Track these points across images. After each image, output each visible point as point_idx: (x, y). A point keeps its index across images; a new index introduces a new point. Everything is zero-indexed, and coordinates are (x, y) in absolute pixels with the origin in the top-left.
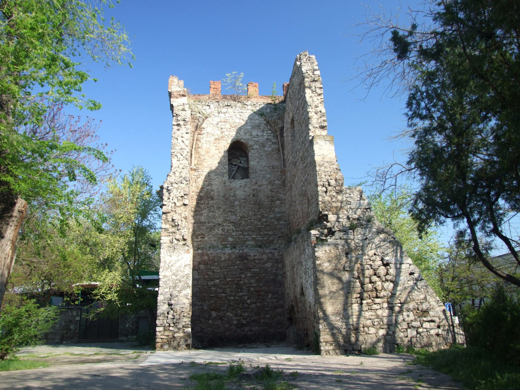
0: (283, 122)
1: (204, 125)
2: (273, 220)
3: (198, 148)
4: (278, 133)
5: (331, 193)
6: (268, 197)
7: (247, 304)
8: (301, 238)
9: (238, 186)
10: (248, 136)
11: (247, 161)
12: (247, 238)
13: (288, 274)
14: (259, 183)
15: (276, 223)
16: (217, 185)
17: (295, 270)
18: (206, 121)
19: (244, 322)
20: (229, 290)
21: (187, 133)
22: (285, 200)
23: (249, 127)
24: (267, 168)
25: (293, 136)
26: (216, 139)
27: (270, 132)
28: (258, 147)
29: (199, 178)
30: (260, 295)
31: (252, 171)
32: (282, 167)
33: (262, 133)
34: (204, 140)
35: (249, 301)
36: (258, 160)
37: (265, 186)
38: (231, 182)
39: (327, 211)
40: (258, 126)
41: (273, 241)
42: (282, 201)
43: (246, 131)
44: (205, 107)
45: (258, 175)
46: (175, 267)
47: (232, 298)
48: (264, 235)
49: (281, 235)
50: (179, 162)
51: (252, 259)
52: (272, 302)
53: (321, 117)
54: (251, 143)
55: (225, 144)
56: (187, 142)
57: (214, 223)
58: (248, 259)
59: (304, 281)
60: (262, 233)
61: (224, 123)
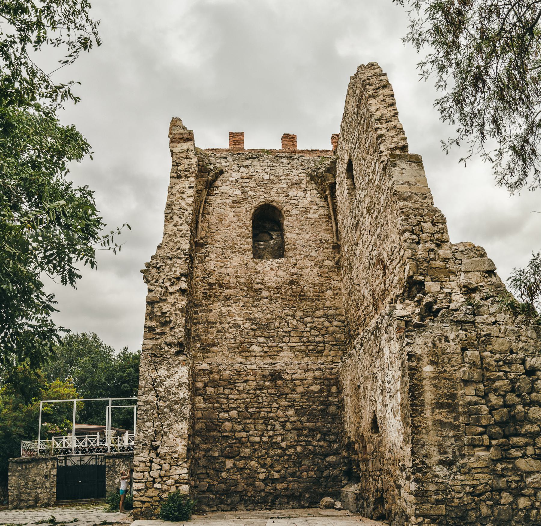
0: (334, 176)
1: (218, 183)
2: (322, 320)
3: (208, 213)
4: (327, 192)
5: (427, 245)
6: (314, 285)
7: (281, 448)
8: (372, 333)
9: (268, 269)
10: (282, 198)
12: (281, 347)
14: (301, 264)
15: (327, 324)
16: (234, 267)
17: (361, 390)
18: (220, 178)
19: (276, 475)
20: (252, 426)
21: (190, 187)
22: (340, 289)
23: (285, 186)
24: (311, 243)
25: (353, 187)
26: (234, 202)
27: (316, 192)
28: (298, 212)
31: (289, 247)
33: (303, 194)
34: (217, 202)
35: (283, 444)
36: (297, 231)
38: (256, 263)
39: (421, 274)
40: (296, 184)
41: (322, 351)
42: (336, 292)
43: (280, 191)
44: (219, 160)
45: (298, 252)
46: (163, 387)
47: (257, 439)
48: (309, 342)
50: (176, 229)
54: (287, 207)
56: (190, 200)
57: (229, 323)
58: (281, 379)
59: (379, 407)
60: (305, 340)
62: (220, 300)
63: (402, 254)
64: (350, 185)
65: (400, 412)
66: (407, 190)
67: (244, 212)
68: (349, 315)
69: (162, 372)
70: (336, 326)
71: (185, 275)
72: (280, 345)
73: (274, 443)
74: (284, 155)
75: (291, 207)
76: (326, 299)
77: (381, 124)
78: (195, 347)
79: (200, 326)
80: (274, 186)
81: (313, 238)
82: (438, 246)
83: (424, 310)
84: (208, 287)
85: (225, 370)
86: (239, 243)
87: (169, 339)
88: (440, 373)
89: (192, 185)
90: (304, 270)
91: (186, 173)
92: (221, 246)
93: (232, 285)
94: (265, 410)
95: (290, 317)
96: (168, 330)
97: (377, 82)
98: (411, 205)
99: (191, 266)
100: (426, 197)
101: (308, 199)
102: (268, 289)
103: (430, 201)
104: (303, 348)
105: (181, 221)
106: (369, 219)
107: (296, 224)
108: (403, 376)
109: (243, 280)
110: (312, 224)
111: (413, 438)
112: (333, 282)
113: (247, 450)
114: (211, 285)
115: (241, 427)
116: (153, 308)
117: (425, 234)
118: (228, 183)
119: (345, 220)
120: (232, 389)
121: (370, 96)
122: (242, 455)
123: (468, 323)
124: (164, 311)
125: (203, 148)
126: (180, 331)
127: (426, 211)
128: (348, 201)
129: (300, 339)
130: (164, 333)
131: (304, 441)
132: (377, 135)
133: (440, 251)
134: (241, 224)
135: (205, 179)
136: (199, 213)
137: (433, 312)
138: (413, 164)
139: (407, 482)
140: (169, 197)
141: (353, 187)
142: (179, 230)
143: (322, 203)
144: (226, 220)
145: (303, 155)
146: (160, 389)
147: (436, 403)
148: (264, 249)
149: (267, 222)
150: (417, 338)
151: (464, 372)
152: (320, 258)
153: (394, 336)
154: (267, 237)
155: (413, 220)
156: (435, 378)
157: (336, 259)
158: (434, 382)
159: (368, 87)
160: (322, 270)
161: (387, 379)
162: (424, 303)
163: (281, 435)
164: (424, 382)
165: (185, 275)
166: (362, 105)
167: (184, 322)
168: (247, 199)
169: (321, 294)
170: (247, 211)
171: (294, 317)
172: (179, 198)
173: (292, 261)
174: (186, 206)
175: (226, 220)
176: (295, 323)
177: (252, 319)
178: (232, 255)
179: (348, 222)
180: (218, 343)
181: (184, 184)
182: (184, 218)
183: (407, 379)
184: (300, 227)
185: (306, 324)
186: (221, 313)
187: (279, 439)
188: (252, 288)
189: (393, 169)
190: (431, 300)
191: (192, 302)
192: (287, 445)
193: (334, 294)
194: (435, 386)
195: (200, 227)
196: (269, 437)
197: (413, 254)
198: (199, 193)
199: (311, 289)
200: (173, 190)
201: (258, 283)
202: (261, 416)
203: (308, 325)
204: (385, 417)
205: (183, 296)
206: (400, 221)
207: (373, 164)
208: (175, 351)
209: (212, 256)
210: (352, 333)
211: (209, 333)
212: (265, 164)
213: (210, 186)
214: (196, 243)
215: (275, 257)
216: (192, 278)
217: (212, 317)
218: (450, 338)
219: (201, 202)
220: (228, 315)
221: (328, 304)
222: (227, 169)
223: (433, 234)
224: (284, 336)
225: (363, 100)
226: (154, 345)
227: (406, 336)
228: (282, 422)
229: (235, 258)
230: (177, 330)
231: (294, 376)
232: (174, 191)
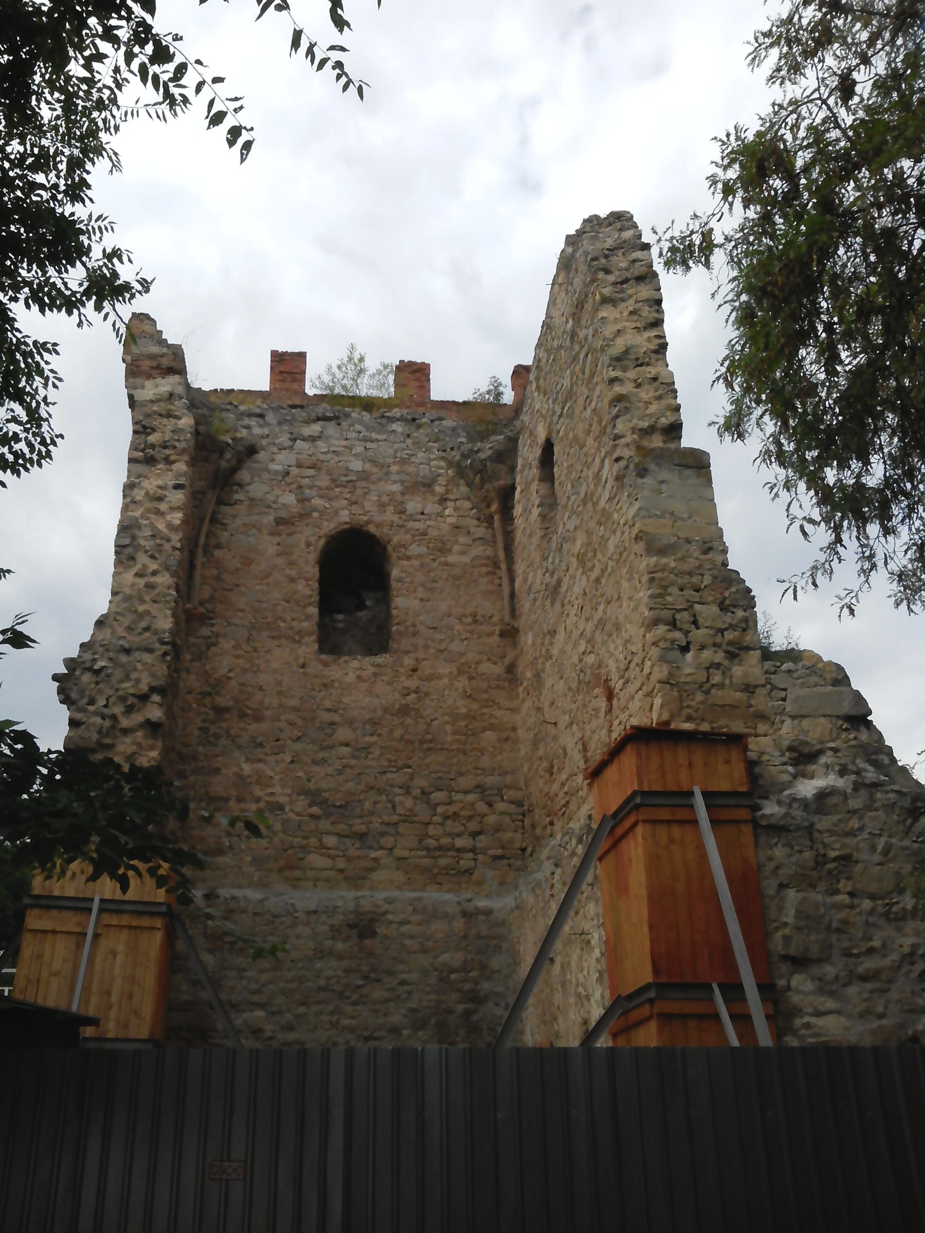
0: (512, 469)
2: (471, 797)
4: (494, 507)
9: (351, 678)
10: (390, 515)
14: (426, 668)
15: (481, 807)
22: (514, 729)
23: (396, 488)
25: (550, 504)
27: (467, 504)
28: (424, 550)
29: (215, 644)
31: (401, 628)
32: (507, 618)
33: (437, 508)
36: (421, 593)
37: (445, 681)
38: (326, 664)
40: (424, 485)
42: (505, 735)
43: (385, 498)
45: (421, 642)
48: (440, 848)
49: (499, 852)
55: (312, 539)
60: (431, 842)
62: (239, 748)
67: (303, 545)
70: (502, 813)
72: (373, 854)
75: (408, 537)
76: (482, 751)
80: (373, 487)
84: (212, 715)
86: (288, 617)
90: (434, 683)
95: (398, 791)
101: (449, 520)
102: (351, 723)
104: (426, 862)
106: (582, 583)
109: (294, 703)
110: (456, 578)
112: (499, 713)
114: (220, 711)
118: (266, 476)
121: (605, 300)
125: (206, 387)
129: (420, 841)
132: (610, 395)
134: (293, 573)
141: (550, 504)
143: (481, 532)
145: (443, 414)
149: (354, 571)
157: (508, 660)
159: (601, 275)
166: (585, 317)
168: (304, 516)
169: (471, 739)
170: (308, 544)
171: (407, 790)
173: (408, 661)
176: (409, 803)
179: (538, 579)
180: (230, 847)
188: (313, 719)
201: (329, 710)
203: (440, 809)
207: (598, 460)
209: (226, 645)
210: (538, 831)
214: (187, 612)
220: (258, 783)
221: (485, 761)
222: (264, 442)
224: (383, 834)
225: (588, 306)
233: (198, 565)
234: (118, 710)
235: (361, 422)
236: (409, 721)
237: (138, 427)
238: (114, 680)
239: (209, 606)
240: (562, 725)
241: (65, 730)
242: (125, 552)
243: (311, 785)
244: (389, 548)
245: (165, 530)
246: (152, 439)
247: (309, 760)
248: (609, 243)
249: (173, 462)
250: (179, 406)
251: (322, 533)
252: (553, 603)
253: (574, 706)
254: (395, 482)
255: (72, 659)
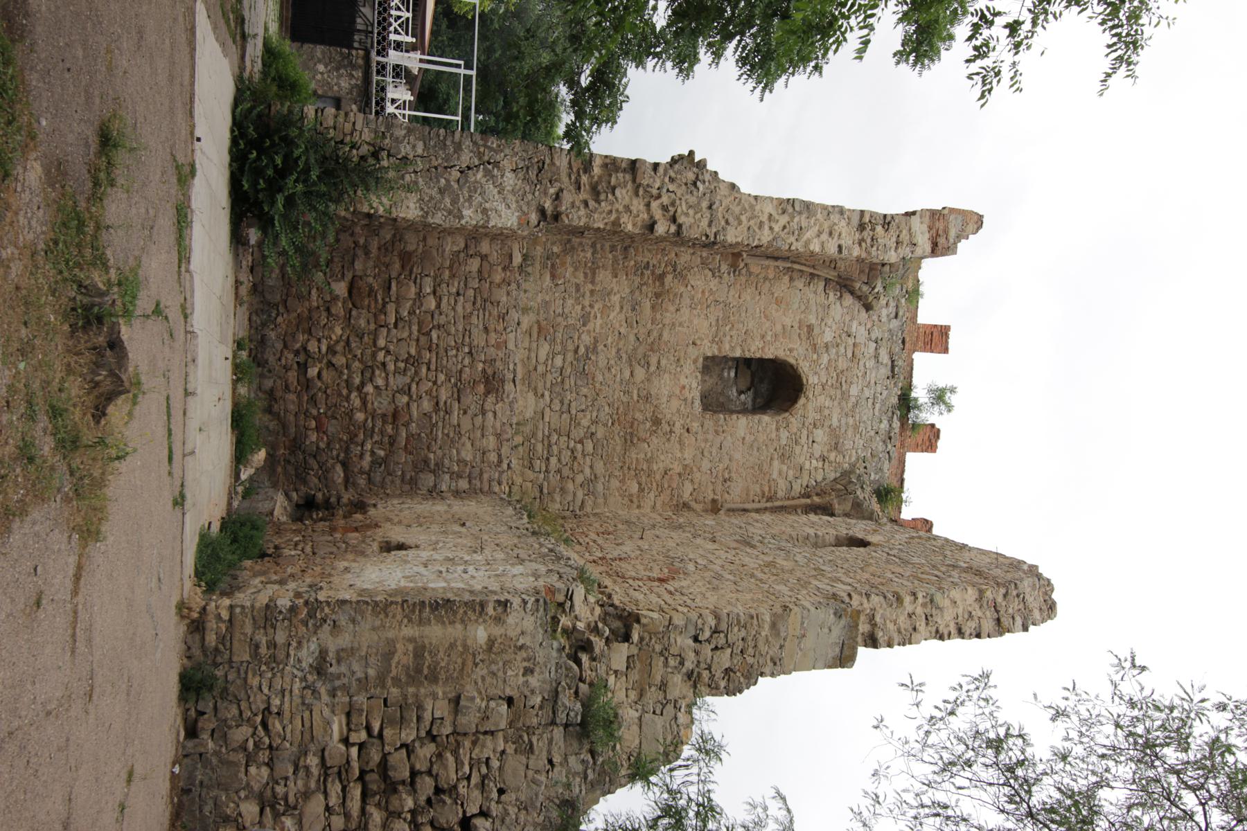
0: (847, 515)
1: (848, 300)
2: (587, 471)
3: (791, 279)
4: (817, 499)
5: (692, 655)
7: (363, 384)
8: (551, 550)
9: (683, 381)
10: (812, 416)
11: (744, 411)
12: (543, 395)
13: (440, 507)
14: (689, 440)
15: (580, 479)
16: (691, 322)
17: (457, 528)
19: (313, 372)
20: (405, 335)
21: (840, 247)
22: (639, 507)
23: (835, 423)
24: (727, 462)
26: (810, 328)
27: (819, 479)
28: (784, 442)
30: (384, 422)
32: (727, 506)
34: (811, 296)
35: (369, 388)
36: (749, 438)
37: (679, 455)
38: (695, 362)
39: (641, 639)
41: (531, 467)
42: (635, 500)
43: (826, 412)
44: (892, 304)
45: (710, 437)
47: (381, 342)
48: (550, 446)
49: (545, 491)
50: (765, 218)
51: (487, 407)
52: (361, 456)
53: (900, 632)
56: (815, 247)
57: (591, 306)
58: (487, 393)
59: (425, 555)
61: (850, 355)
63: (680, 608)
64: (824, 540)
65: (412, 585)
66: (791, 631)
67: (790, 346)
68: (592, 518)
69: (509, 179)
70: (575, 494)
71: (678, 233)
72: (547, 394)
73: (373, 373)
74: (894, 425)
76: (622, 481)
77: (924, 605)
78: (553, 244)
79: (589, 255)
80: (836, 403)
81: (734, 466)
82: (689, 675)
83: (580, 637)
84: (658, 272)
85: (508, 294)
86: (733, 333)
87: (567, 198)
88: (474, 655)
89: (845, 252)
91: (869, 241)
92: (731, 299)
93: (658, 316)
94: (434, 360)
95: (595, 414)
96: (584, 195)
97: (1010, 611)
98: (763, 634)
99: (694, 244)
100: (775, 664)
101: (807, 463)
103: (767, 670)
104: (540, 435)
105: (777, 228)
107: (762, 437)
108: (471, 592)
110: (760, 467)
111: (367, 603)
112: (652, 495)
113: (362, 323)
114: (661, 277)
115: (406, 314)
116: (625, 171)
117: (710, 654)
118: (848, 318)
119: (759, 526)
120: (474, 303)
122: (354, 313)
123: (554, 713)
124: (617, 192)
126: (579, 218)
127: (750, 660)
128: (794, 534)
130: (579, 188)
131: (374, 426)
133: (680, 677)
135: (856, 275)
136: (793, 262)
137: (576, 653)
138: (838, 650)
139: (292, 594)
140: (825, 207)
142: (761, 225)
143: (797, 488)
144: (777, 311)
145: (895, 462)
146: (480, 175)
147: (424, 647)
148: (721, 377)
150: (532, 619)
151: (473, 699)
152: (698, 475)
153: (541, 583)
154: (744, 384)
155: (736, 635)
156: (465, 646)
157: (693, 504)
158: (458, 643)
160: (676, 478)
161: (471, 569)
162: (592, 638)
163: (387, 385)
164: (459, 626)
165: (678, 233)
167: (596, 226)
168: (815, 350)
169: (633, 473)
170: (791, 350)
171: (595, 422)
172: (821, 226)
173: (695, 426)
174: (805, 238)
175: (777, 311)
176: (585, 422)
177: (595, 347)
178: (713, 319)
179: (756, 531)
180: (557, 285)
181: (848, 237)
182: (783, 234)
183: (467, 597)
184: (756, 445)
185: (581, 442)
186: (609, 294)
187: (380, 382)
188: (652, 350)
189: (832, 611)
190: (597, 650)
191: (633, 242)
192: (367, 394)
193: (631, 495)
194: (452, 646)
195: (767, 262)
196: (384, 364)
197: (676, 627)
198: (832, 263)
199: (642, 456)
200: (838, 216)
201: (659, 362)
202: (423, 352)
203: (579, 446)
204: (406, 562)
205: (642, 227)
206: (736, 611)
208: (546, 206)
209: (713, 284)
210: (561, 521)
211: (576, 269)
212: (879, 390)
213: (844, 285)
215: (704, 397)
216: (675, 244)
217: (604, 276)
218: (530, 678)
219: (813, 267)
220: (605, 306)
222: (875, 318)
223: (709, 668)
224: (562, 402)
226: (558, 168)
227: (537, 601)
228: (409, 389)
229: (706, 324)
230: (582, 212)
231: (490, 415)
232: (835, 218)
233: (776, 264)
234: (665, 199)
235: (889, 395)
236: (648, 425)
237: (888, 219)
238: (688, 196)
239: (744, 271)
240: (640, 543)
241: (652, 159)
242: (788, 206)
243: (601, 347)
244: (787, 414)
245: (805, 238)
246: (879, 229)
247: (620, 346)
248: (1029, 599)
249: (860, 245)
250: (905, 251)
251: (800, 361)
252: (737, 541)
253: (654, 552)
254: (840, 421)
255: (705, 166)
